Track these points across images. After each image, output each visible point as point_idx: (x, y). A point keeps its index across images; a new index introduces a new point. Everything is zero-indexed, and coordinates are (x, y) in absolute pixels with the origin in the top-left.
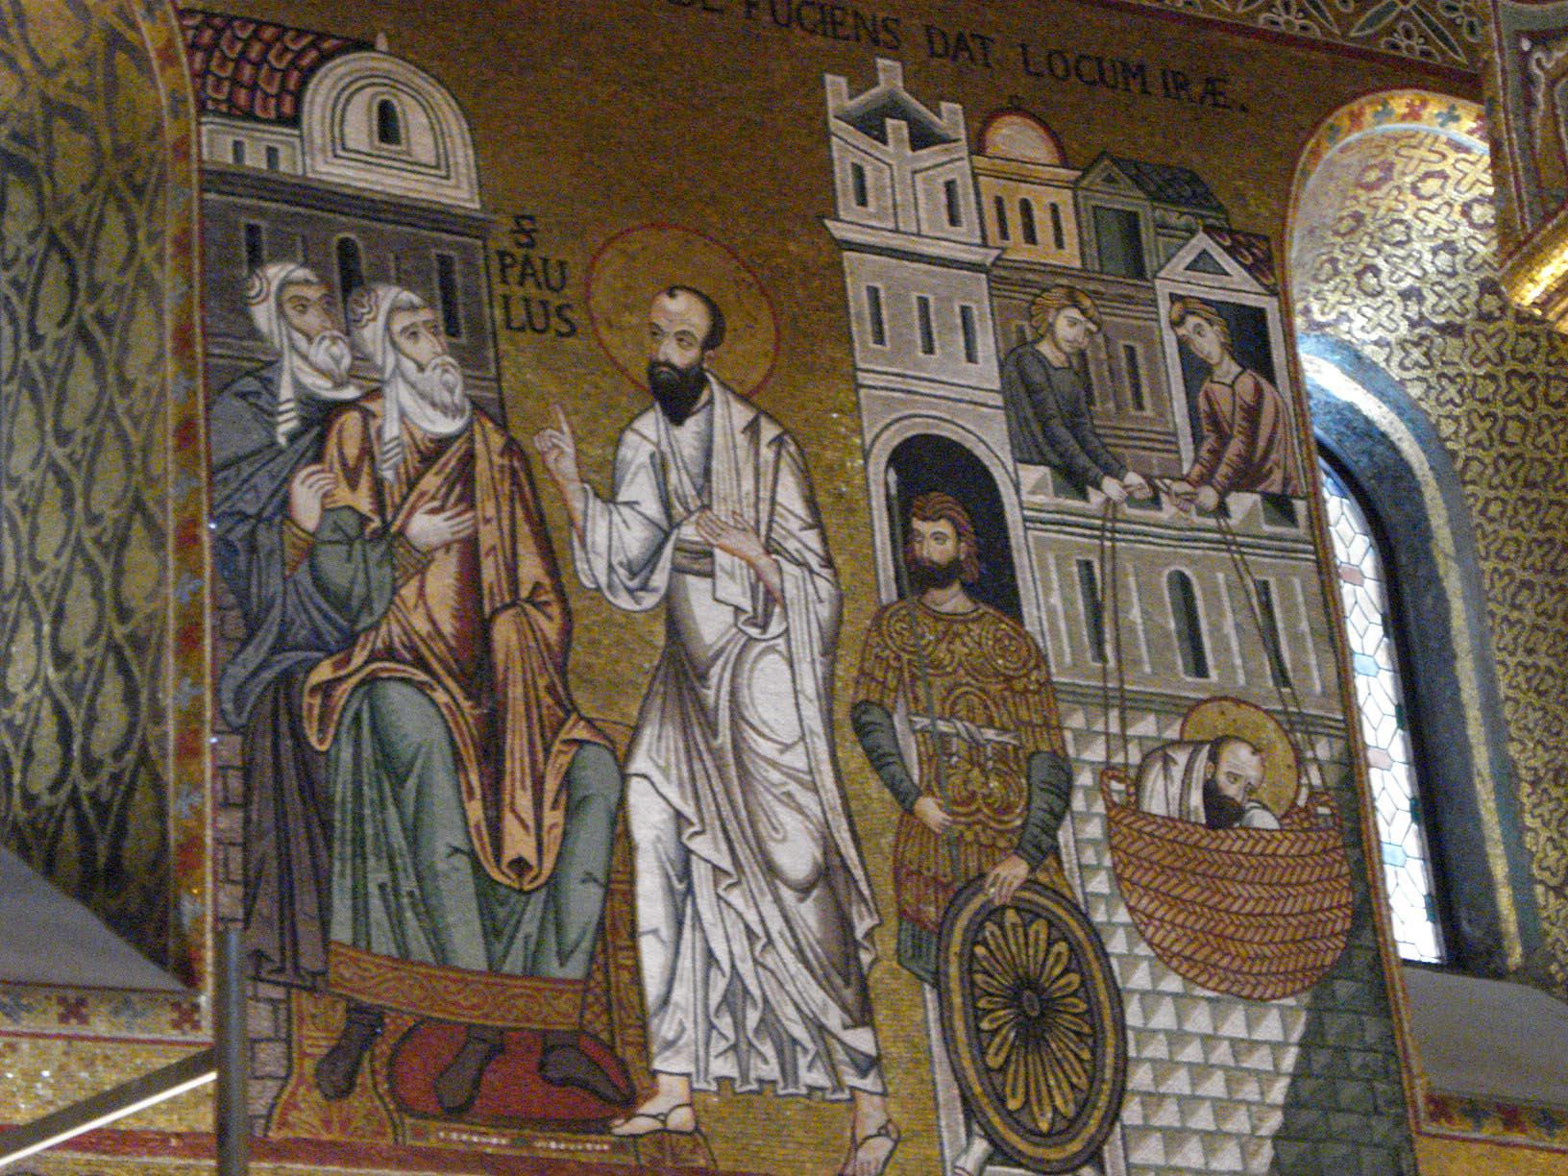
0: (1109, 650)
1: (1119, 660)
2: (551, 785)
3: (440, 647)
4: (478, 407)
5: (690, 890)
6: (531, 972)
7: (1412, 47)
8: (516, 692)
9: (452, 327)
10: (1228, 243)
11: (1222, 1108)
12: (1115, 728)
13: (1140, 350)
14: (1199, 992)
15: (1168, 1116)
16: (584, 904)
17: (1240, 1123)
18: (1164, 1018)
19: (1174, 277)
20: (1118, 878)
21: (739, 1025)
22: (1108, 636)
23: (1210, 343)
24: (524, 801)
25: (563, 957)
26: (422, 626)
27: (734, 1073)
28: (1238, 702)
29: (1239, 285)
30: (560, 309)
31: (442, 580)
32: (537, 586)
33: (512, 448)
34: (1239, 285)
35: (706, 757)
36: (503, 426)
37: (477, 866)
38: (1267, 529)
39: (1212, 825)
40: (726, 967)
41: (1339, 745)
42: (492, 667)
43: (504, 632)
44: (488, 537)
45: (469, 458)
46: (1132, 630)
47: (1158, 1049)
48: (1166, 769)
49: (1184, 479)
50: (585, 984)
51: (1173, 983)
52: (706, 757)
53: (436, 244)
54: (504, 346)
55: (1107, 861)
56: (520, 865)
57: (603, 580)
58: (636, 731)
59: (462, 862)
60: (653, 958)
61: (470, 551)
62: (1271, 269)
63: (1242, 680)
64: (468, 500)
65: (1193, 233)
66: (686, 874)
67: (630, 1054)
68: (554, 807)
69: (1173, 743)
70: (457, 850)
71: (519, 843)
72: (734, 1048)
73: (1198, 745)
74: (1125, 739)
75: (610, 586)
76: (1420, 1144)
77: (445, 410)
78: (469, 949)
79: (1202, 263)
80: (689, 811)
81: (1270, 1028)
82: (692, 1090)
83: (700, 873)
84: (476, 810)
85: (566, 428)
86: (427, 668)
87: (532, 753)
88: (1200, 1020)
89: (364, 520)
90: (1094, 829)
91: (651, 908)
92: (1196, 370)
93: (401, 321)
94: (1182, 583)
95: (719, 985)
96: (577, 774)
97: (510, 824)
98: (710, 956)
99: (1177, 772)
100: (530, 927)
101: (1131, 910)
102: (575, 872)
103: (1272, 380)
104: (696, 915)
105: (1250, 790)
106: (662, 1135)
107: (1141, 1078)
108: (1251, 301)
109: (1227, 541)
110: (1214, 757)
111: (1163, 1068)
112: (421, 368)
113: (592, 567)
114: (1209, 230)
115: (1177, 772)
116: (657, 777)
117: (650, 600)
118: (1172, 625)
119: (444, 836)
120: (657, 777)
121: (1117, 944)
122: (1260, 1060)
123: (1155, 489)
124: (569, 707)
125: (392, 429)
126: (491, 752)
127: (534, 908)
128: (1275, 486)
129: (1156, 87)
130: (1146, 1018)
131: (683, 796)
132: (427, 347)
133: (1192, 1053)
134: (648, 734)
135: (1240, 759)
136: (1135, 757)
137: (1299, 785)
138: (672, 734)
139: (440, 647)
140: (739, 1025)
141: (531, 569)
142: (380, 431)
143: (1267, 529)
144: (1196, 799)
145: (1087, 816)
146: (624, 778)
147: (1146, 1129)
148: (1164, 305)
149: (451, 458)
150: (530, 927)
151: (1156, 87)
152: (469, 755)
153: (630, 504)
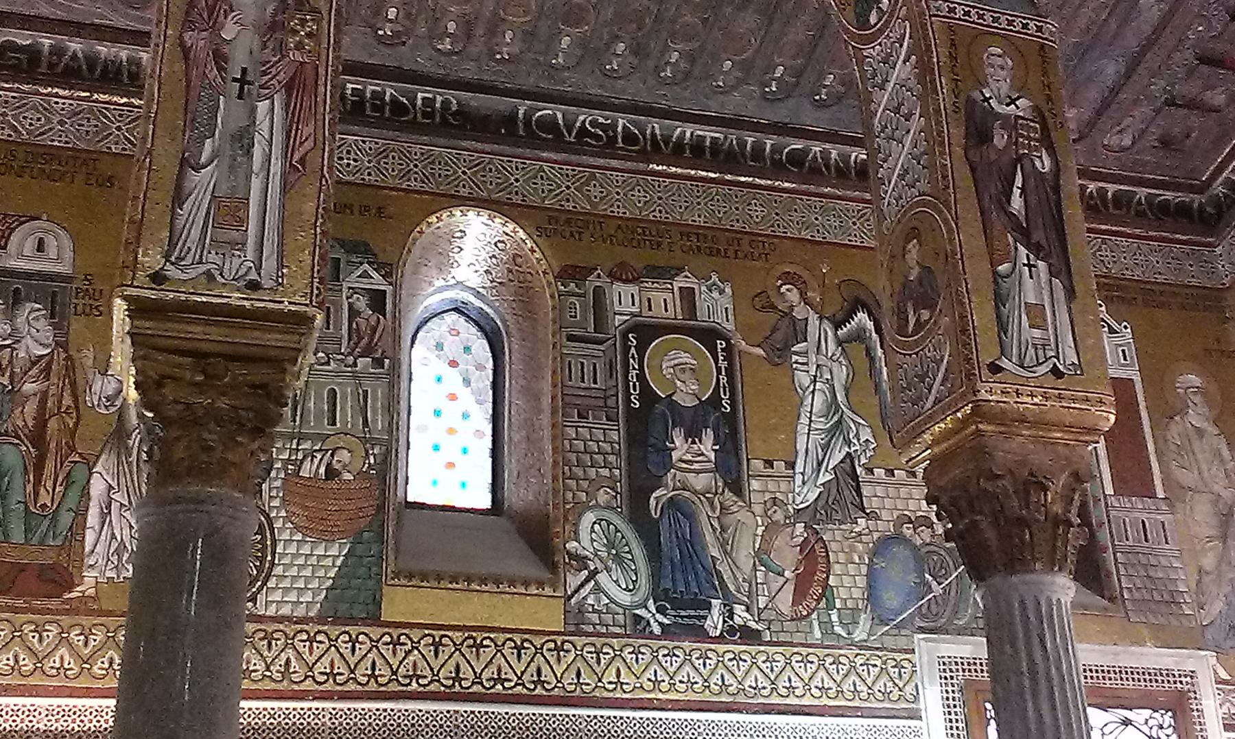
0: (298, 418)
1: (301, 422)
2: (60, 479)
3: (27, 431)
4: (57, 343)
5: (110, 512)
6: (42, 543)
7: (464, 192)
8: (53, 445)
9: (52, 316)
10: (376, 266)
11: (307, 580)
12: (294, 446)
13: (332, 310)
14: (308, 539)
15: (286, 584)
16: (66, 519)
17: (315, 584)
18: (292, 549)
19: (352, 280)
20: (283, 499)
21: (120, 559)
22: (299, 413)
23: (362, 303)
24: (49, 484)
25: (54, 538)
26: (21, 424)
27: (115, 576)
28: (346, 434)
29: (377, 281)
30: (96, 307)
31: (31, 408)
32: (68, 407)
33: (69, 358)
34: (377, 281)
35: (126, 466)
36: (66, 351)
37: (27, 508)
38: (373, 371)
39: (327, 479)
40: (119, 538)
41: (384, 448)
42: (45, 438)
43: (53, 424)
44: (52, 391)
45: (49, 364)
46: (310, 412)
47: (286, 561)
48: (312, 460)
49: (342, 354)
50: (61, 547)
51: (299, 537)
52: (126, 466)
53: (51, 286)
54: (72, 321)
55: (281, 495)
56: (44, 506)
57: (96, 403)
58: (98, 457)
59: (22, 507)
60: (90, 537)
61: (44, 396)
62: (392, 276)
63: (349, 426)
64: (47, 378)
65: (361, 264)
66: (109, 506)
67: (75, 571)
68: (61, 485)
69: (316, 451)
70: (20, 502)
71: (45, 498)
72: (116, 567)
73: (327, 451)
74: (298, 450)
75: (98, 405)
76: (385, 589)
77: (45, 346)
78: (18, 536)
79: (365, 275)
80: (114, 484)
81: (334, 551)
82: (97, 582)
83: (114, 506)
84: (30, 488)
85: (92, 349)
86: (19, 439)
87: (56, 468)
88: (306, 550)
89: (5, 386)
90: (278, 483)
91: (93, 518)
92: (353, 313)
93: (34, 315)
94: (333, 393)
95: (115, 545)
96: (73, 473)
97: (42, 490)
98: (113, 536)
99: (316, 461)
100: (44, 528)
101: (287, 512)
102: (65, 507)
103: (384, 316)
104: (111, 521)
105: (345, 466)
106: (83, 598)
107: (278, 570)
108: (382, 288)
109: (355, 376)
110: (332, 455)
111: (287, 567)
112: (38, 331)
113: (92, 399)
114: (369, 263)
115: (316, 461)
116: (104, 473)
117: (113, 409)
118: (326, 408)
119: (16, 496)
120: (104, 473)
121: (278, 524)
122: (329, 562)
123: (329, 358)
124: (72, 449)
125: (22, 355)
126: (39, 467)
127: (46, 522)
128: (378, 355)
129: (356, 212)
130: (285, 549)
131: (113, 480)
132: (42, 324)
133: (301, 561)
134: (103, 457)
135: (344, 455)
136: (300, 456)
137: (364, 463)
138: (114, 459)
139: (27, 431)
140: (120, 559)
141: (67, 401)
142: (17, 354)
143: (373, 371)
144: (322, 470)
145: (276, 479)
146: (91, 474)
147: (277, 588)
148: (345, 290)
149: (43, 363)
150: (44, 528)
151: (356, 212)
152: (31, 469)
153: (112, 375)
